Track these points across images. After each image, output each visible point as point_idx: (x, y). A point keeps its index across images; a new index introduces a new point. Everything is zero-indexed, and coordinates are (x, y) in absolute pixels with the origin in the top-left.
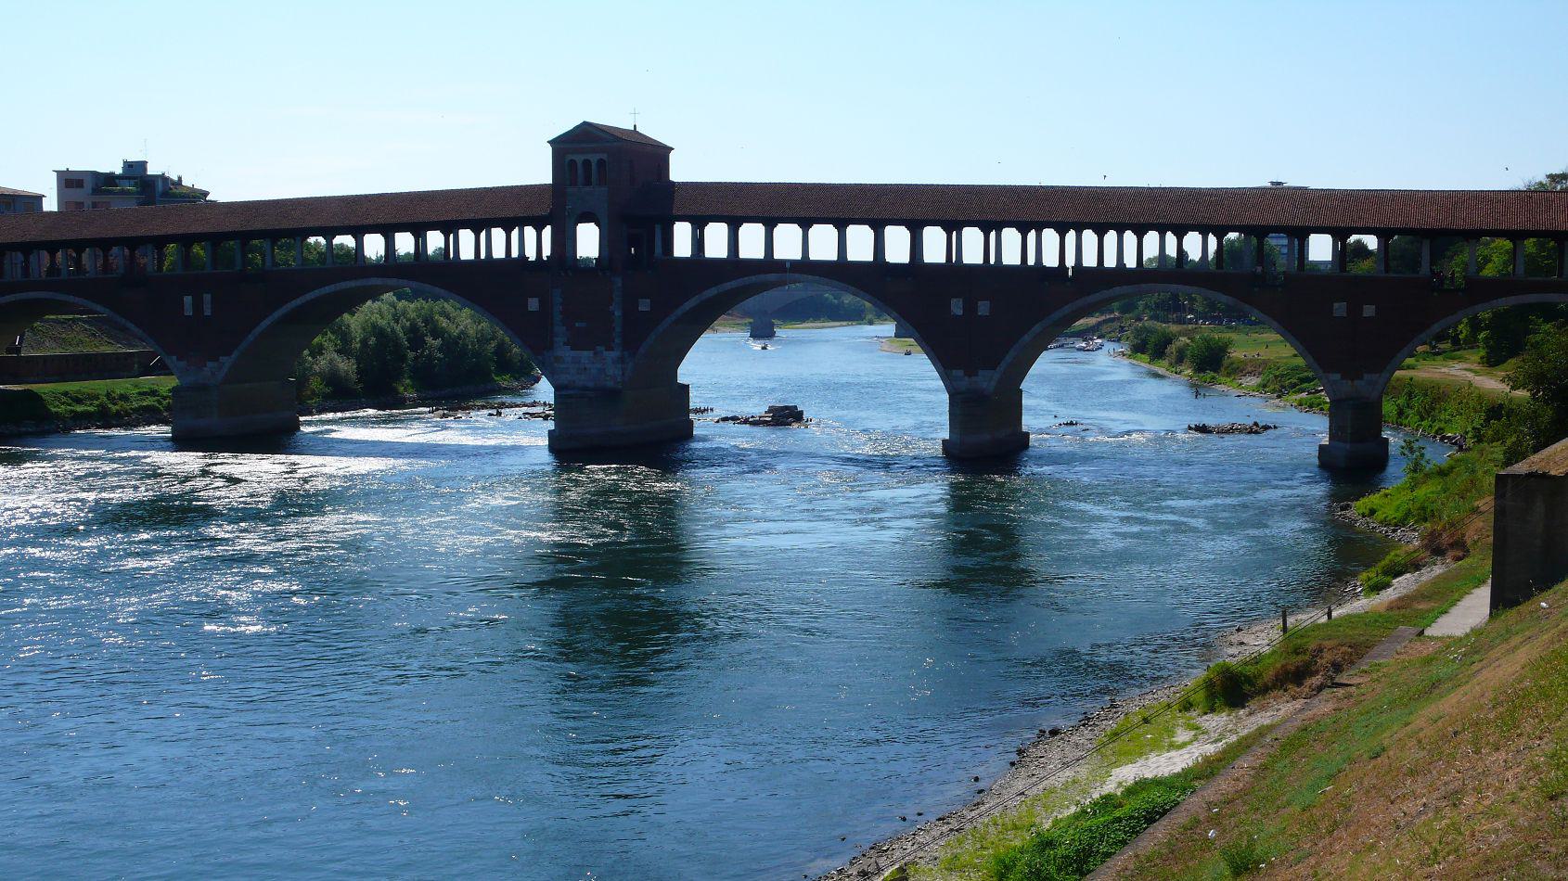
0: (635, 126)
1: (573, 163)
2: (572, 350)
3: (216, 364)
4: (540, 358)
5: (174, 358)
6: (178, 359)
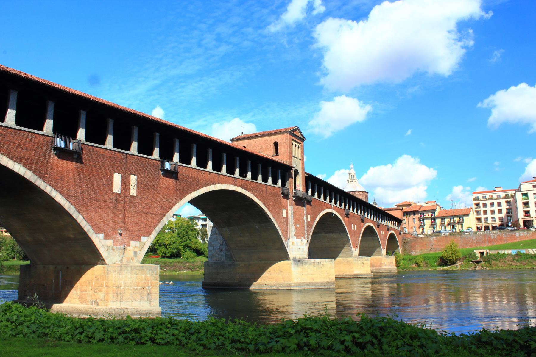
0: (242, 133)
1: (292, 144)
2: (296, 238)
3: (137, 244)
4: (286, 242)
5: (101, 236)
6: (106, 238)
